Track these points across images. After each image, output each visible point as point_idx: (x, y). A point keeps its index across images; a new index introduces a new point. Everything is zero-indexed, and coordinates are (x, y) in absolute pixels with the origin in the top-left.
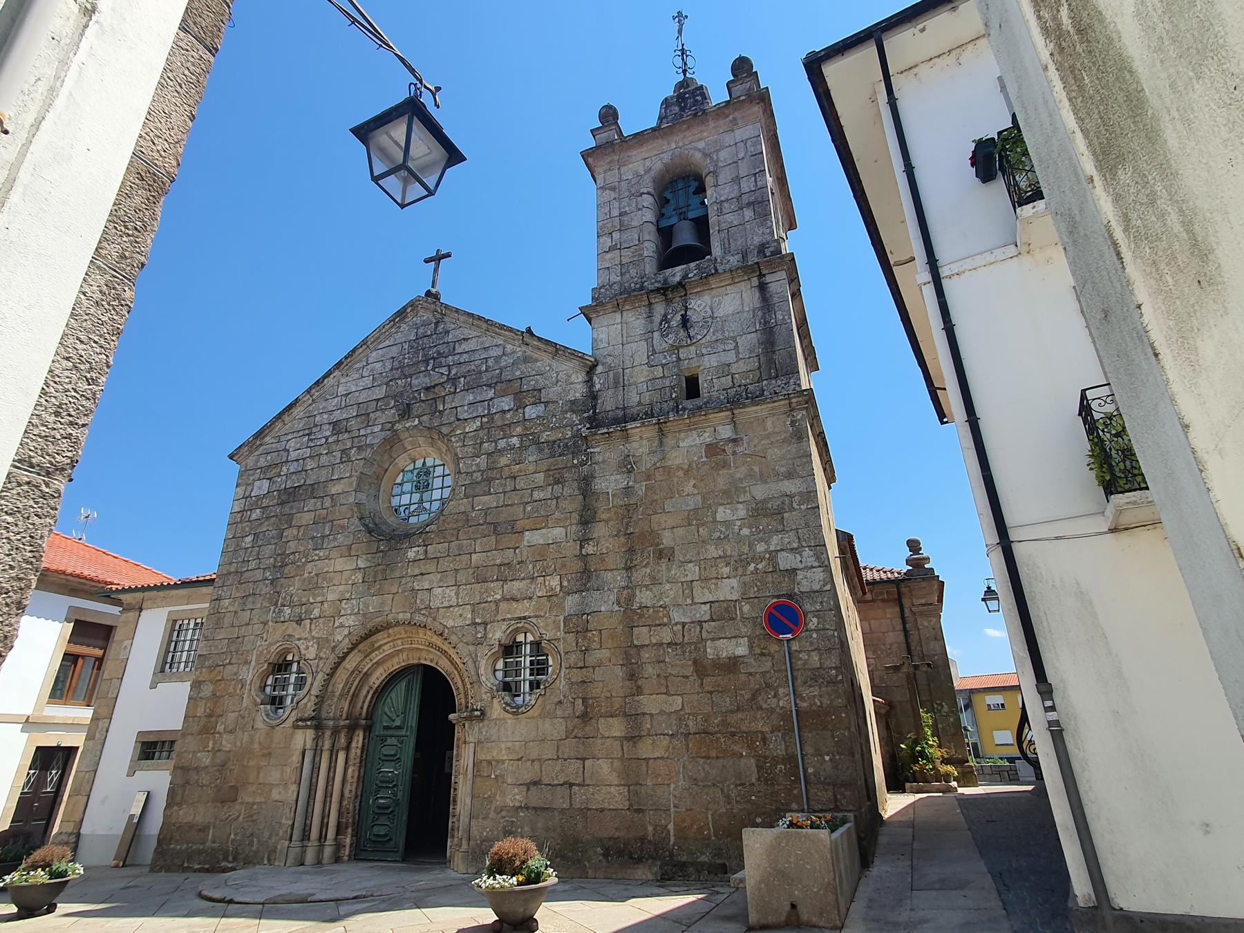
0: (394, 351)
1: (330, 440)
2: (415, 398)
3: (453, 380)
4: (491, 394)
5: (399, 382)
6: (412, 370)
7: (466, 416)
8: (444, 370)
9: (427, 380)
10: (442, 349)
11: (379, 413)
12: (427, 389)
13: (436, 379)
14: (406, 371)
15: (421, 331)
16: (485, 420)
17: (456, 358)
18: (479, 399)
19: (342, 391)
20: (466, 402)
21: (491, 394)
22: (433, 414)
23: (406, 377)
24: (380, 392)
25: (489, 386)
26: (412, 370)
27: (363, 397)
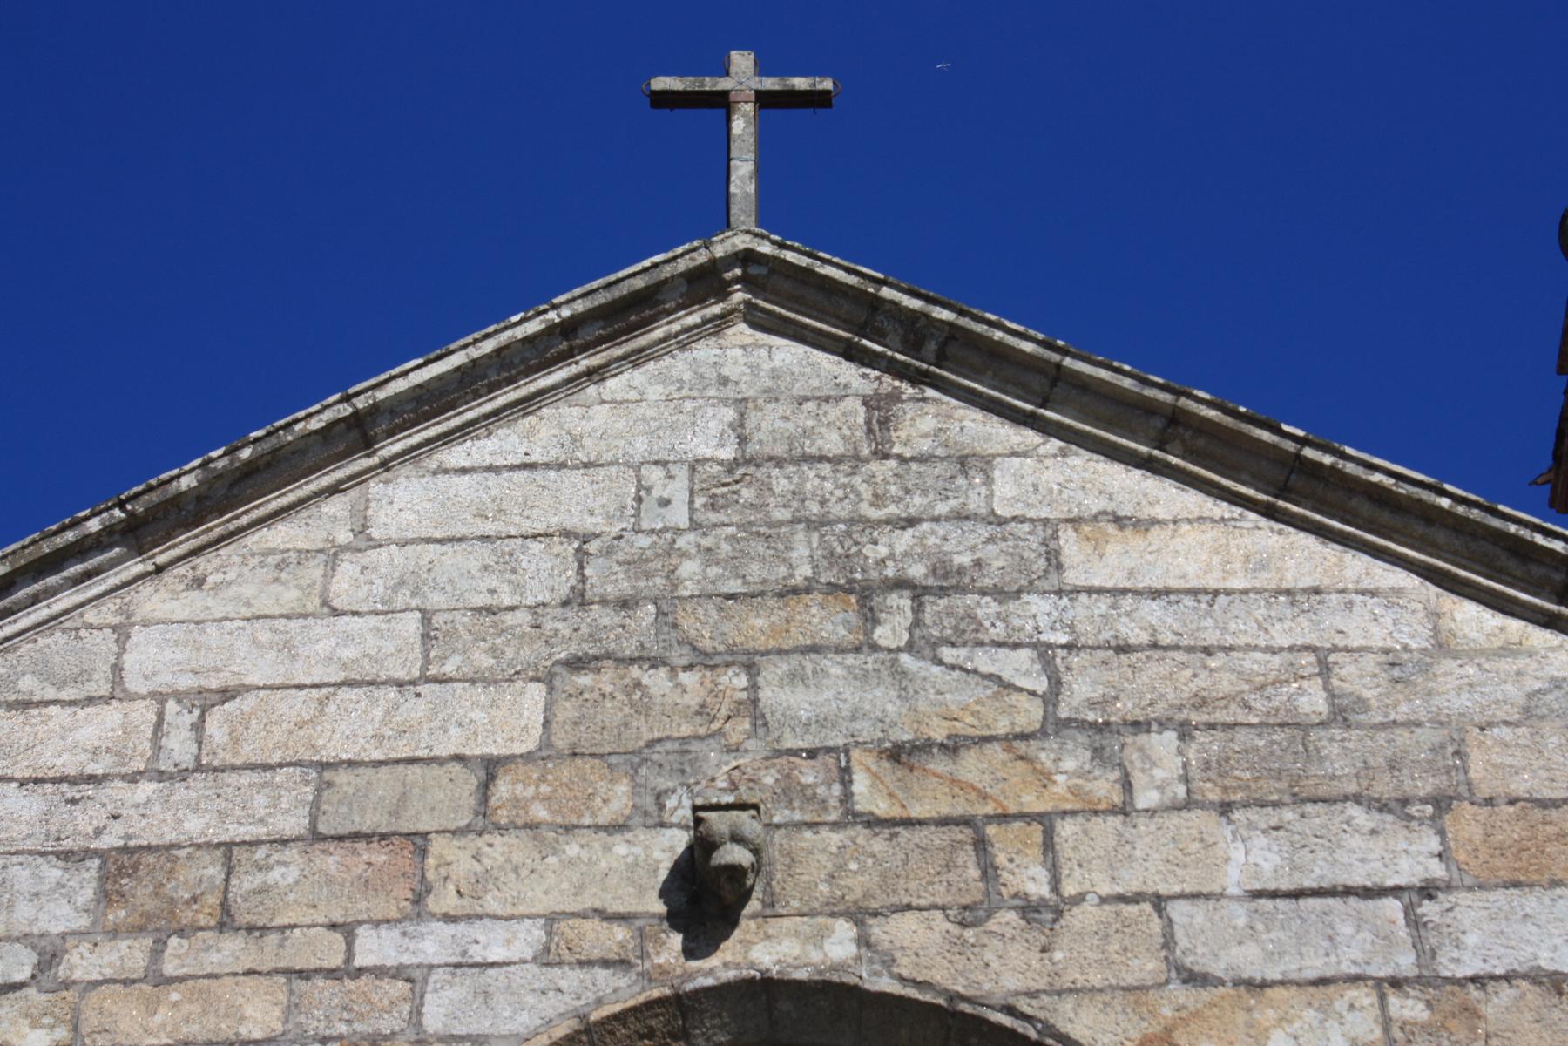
0: (580, 502)
1: (82, 964)
2: (790, 791)
3: (1105, 735)
4: (1412, 856)
5: (658, 681)
6: (757, 626)
7: (1248, 959)
8: (1019, 666)
9: (883, 699)
10: (962, 547)
11: (498, 849)
12: (897, 754)
13: (940, 697)
14: (702, 625)
15: (770, 425)
16: (1408, 1008)
17: (1084, 611)
18: (1318, 873)
19: (153, 659)
20: (1233, 879)
21: (1412, 856)
22: (970, 916)
23: (704, 660)
24: (513, 720)
25: (1399, 807)
26: (757, 626)
27: (350, 729)
